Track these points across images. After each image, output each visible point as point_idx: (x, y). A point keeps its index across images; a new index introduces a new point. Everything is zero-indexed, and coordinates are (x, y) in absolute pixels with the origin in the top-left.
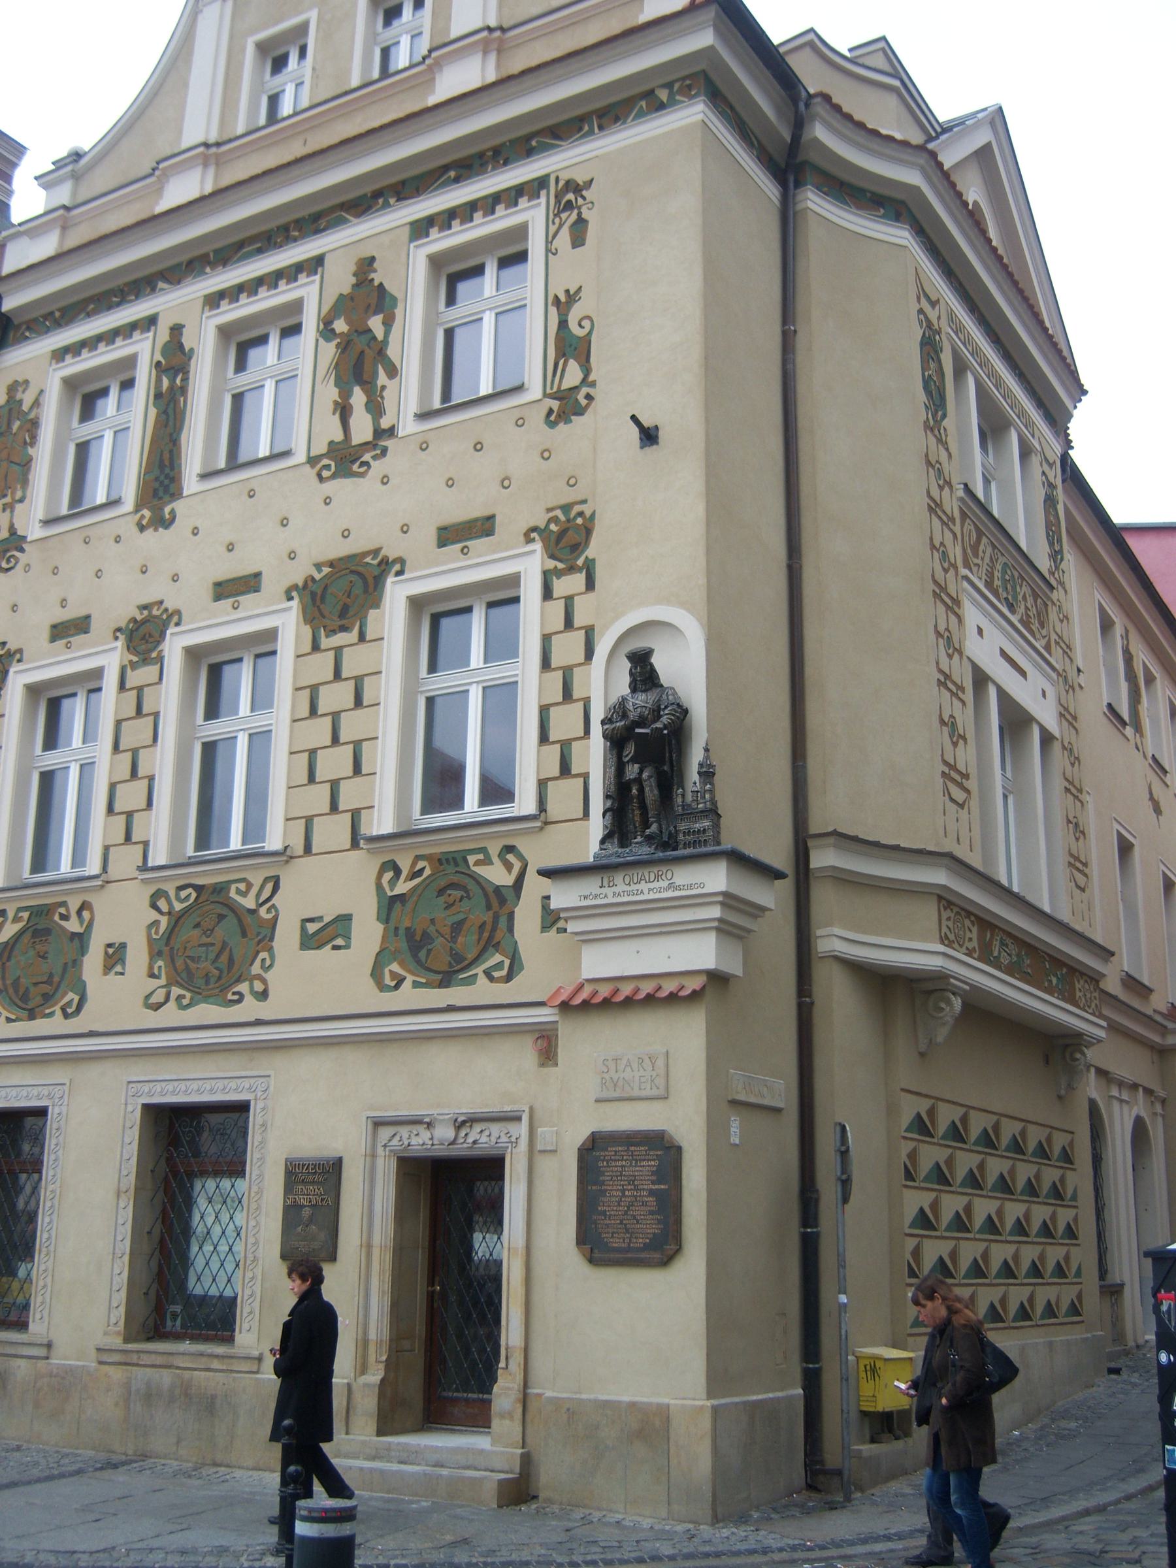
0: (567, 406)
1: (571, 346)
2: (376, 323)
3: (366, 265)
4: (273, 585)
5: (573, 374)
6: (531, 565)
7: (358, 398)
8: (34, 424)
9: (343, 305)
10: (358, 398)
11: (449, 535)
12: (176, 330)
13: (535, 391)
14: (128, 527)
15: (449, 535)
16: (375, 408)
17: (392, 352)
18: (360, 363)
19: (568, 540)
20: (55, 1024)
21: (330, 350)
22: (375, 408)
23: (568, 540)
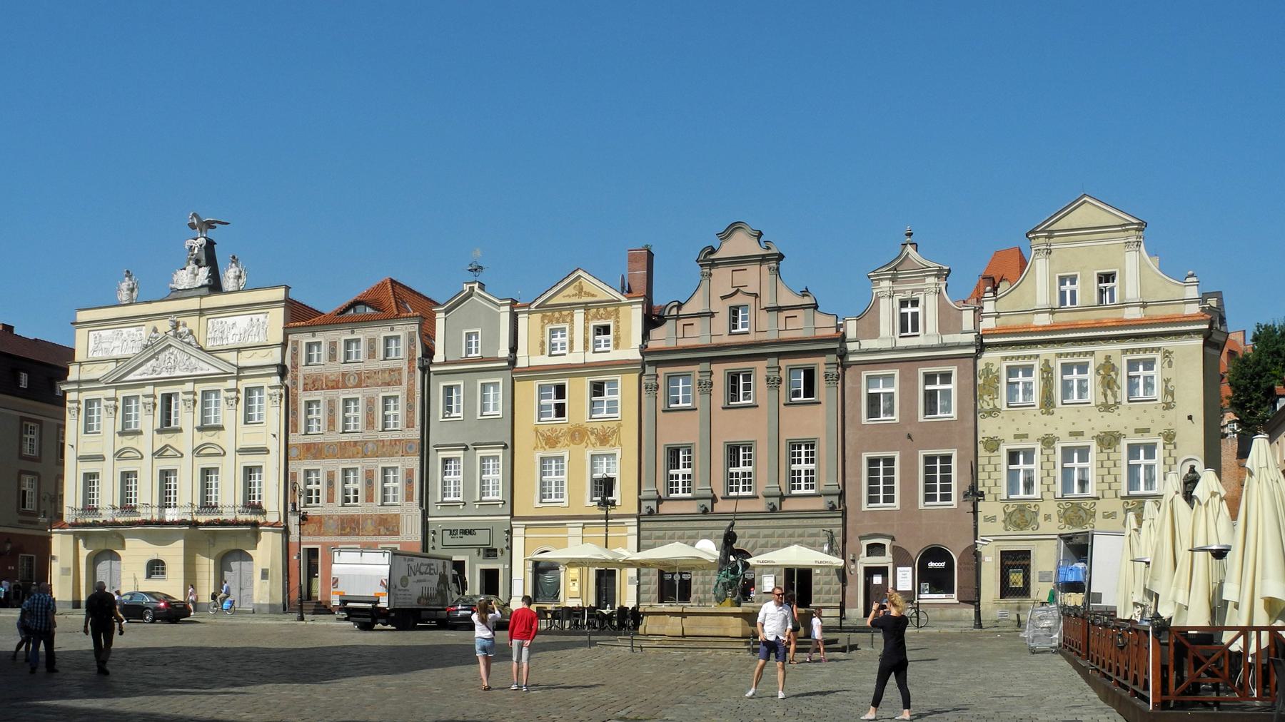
0: (1168, 406)
1: (1168, 392)
2: (1113, 374)
3: (1108, 358)
4: (1088, 434)
5: (1169, 399)
6: (1160, 441)
7: (1109, 392)
8: (998, 377)
9: (1102, 366)
10: (1109, 392)
11: (1137, 431)
12: (1047, 361)
13: (1160, 401)
14: (1038, 413)
15: (1137, 431)
16: (1115, 396)
17: (1118, 382)
18: (1109, 384)
19: (1169, 437)
20: (1030, 531)
21: (1099, 378)
22: (1115, 396)
23: (1169, 437)
